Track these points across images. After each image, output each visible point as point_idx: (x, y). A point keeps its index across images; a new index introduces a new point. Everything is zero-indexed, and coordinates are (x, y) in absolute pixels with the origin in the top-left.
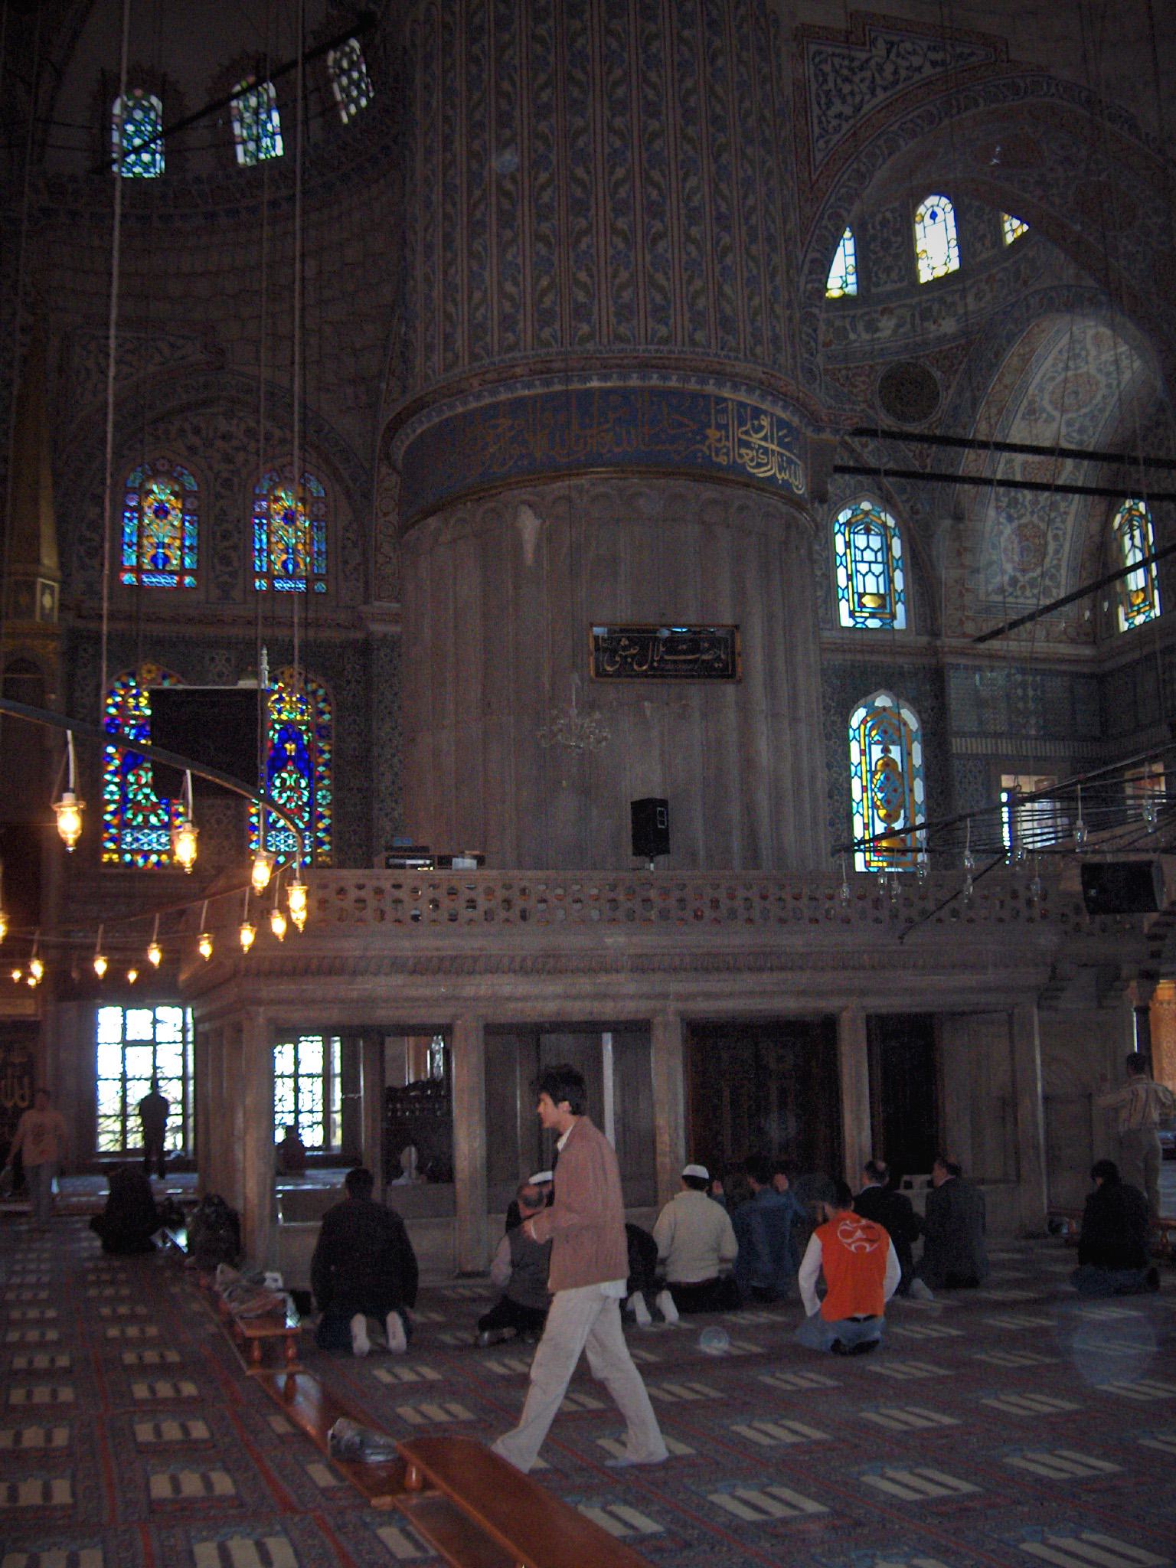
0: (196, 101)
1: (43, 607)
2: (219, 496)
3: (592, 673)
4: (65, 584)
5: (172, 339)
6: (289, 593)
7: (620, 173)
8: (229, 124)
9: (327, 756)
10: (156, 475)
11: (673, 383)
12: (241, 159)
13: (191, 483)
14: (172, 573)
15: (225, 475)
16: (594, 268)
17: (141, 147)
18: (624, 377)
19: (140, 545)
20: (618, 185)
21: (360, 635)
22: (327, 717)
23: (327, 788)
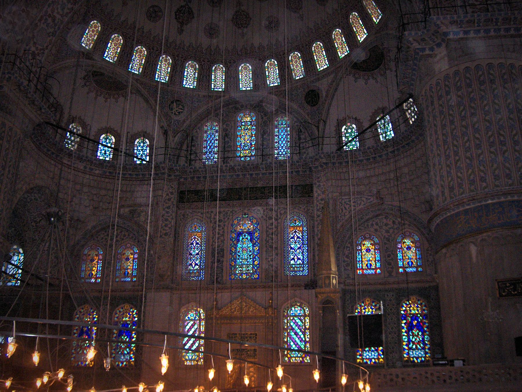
0: (366, 125)
1: (333, 283)
2: (385, 244)
3: (498, 296)
4: (340, 276)
5: (366, 197)
6: (411, 272)
7: (490, 133)
8: (377, 129)
9: (427, 324)
10: (365, 239)
11: (516, 198)
12: (381, 139)
13: (376, 240)
14: (373, 269)
15: (387, 236)
16: (485, 165)
17: (351, 140)
18: (499, 198)
19: (362, 261)
20: (490, 137)
21: (434, 284)
22: (426, 311)
23: (427, 335)
